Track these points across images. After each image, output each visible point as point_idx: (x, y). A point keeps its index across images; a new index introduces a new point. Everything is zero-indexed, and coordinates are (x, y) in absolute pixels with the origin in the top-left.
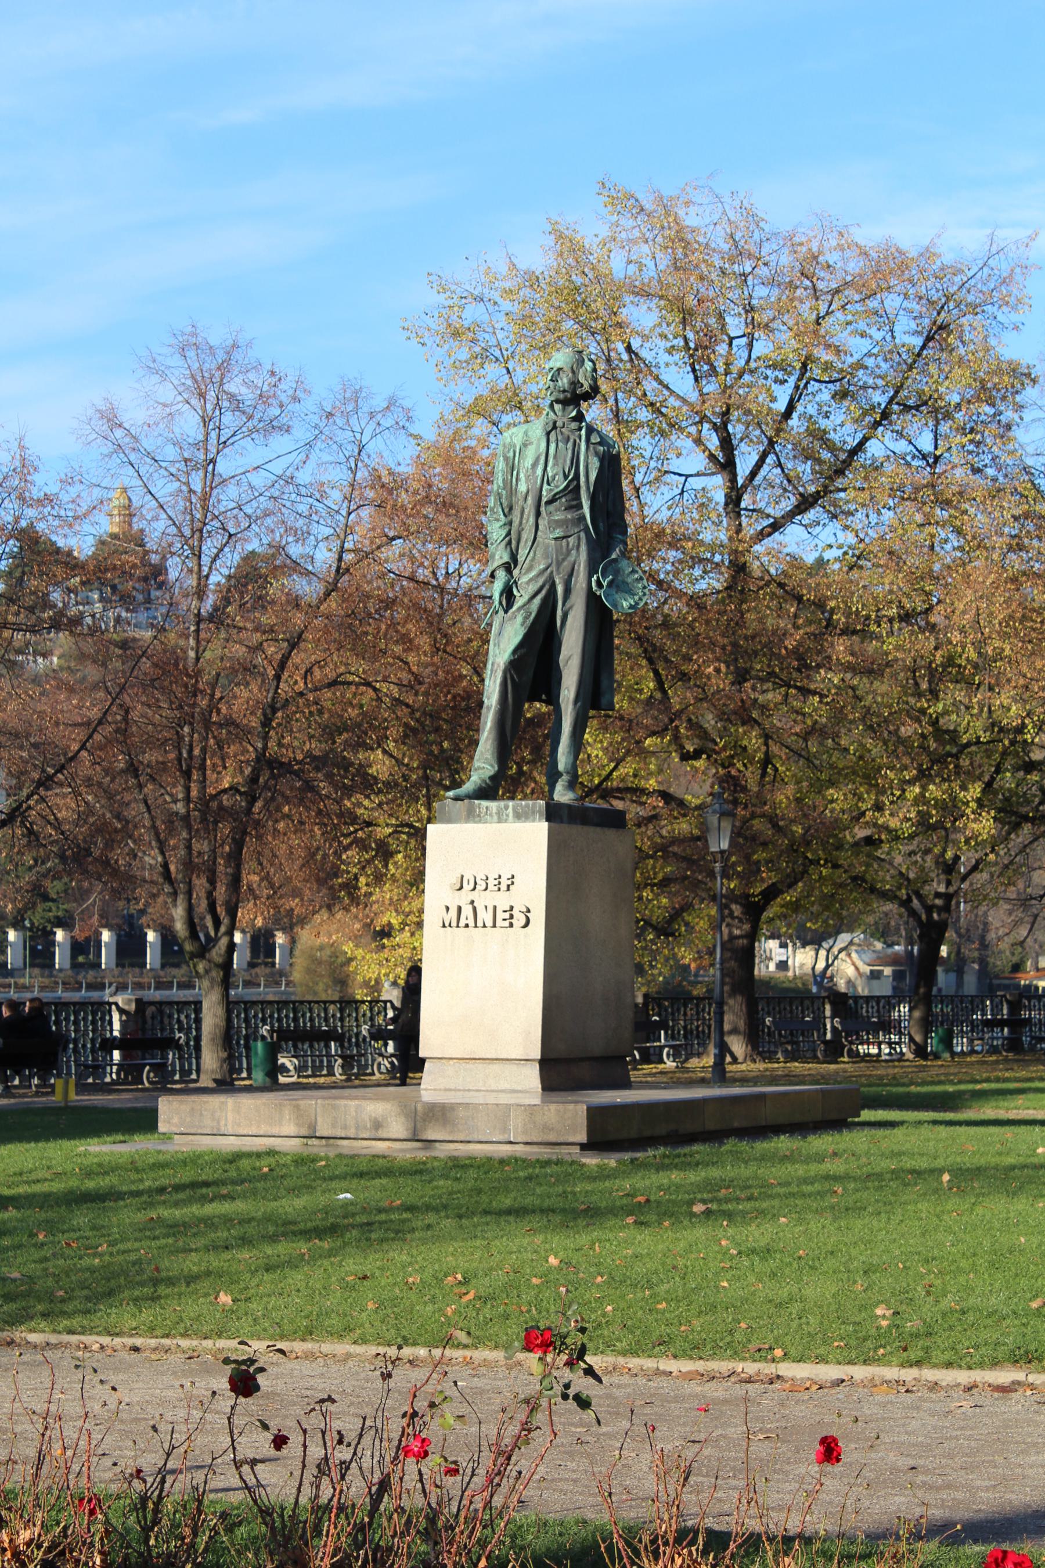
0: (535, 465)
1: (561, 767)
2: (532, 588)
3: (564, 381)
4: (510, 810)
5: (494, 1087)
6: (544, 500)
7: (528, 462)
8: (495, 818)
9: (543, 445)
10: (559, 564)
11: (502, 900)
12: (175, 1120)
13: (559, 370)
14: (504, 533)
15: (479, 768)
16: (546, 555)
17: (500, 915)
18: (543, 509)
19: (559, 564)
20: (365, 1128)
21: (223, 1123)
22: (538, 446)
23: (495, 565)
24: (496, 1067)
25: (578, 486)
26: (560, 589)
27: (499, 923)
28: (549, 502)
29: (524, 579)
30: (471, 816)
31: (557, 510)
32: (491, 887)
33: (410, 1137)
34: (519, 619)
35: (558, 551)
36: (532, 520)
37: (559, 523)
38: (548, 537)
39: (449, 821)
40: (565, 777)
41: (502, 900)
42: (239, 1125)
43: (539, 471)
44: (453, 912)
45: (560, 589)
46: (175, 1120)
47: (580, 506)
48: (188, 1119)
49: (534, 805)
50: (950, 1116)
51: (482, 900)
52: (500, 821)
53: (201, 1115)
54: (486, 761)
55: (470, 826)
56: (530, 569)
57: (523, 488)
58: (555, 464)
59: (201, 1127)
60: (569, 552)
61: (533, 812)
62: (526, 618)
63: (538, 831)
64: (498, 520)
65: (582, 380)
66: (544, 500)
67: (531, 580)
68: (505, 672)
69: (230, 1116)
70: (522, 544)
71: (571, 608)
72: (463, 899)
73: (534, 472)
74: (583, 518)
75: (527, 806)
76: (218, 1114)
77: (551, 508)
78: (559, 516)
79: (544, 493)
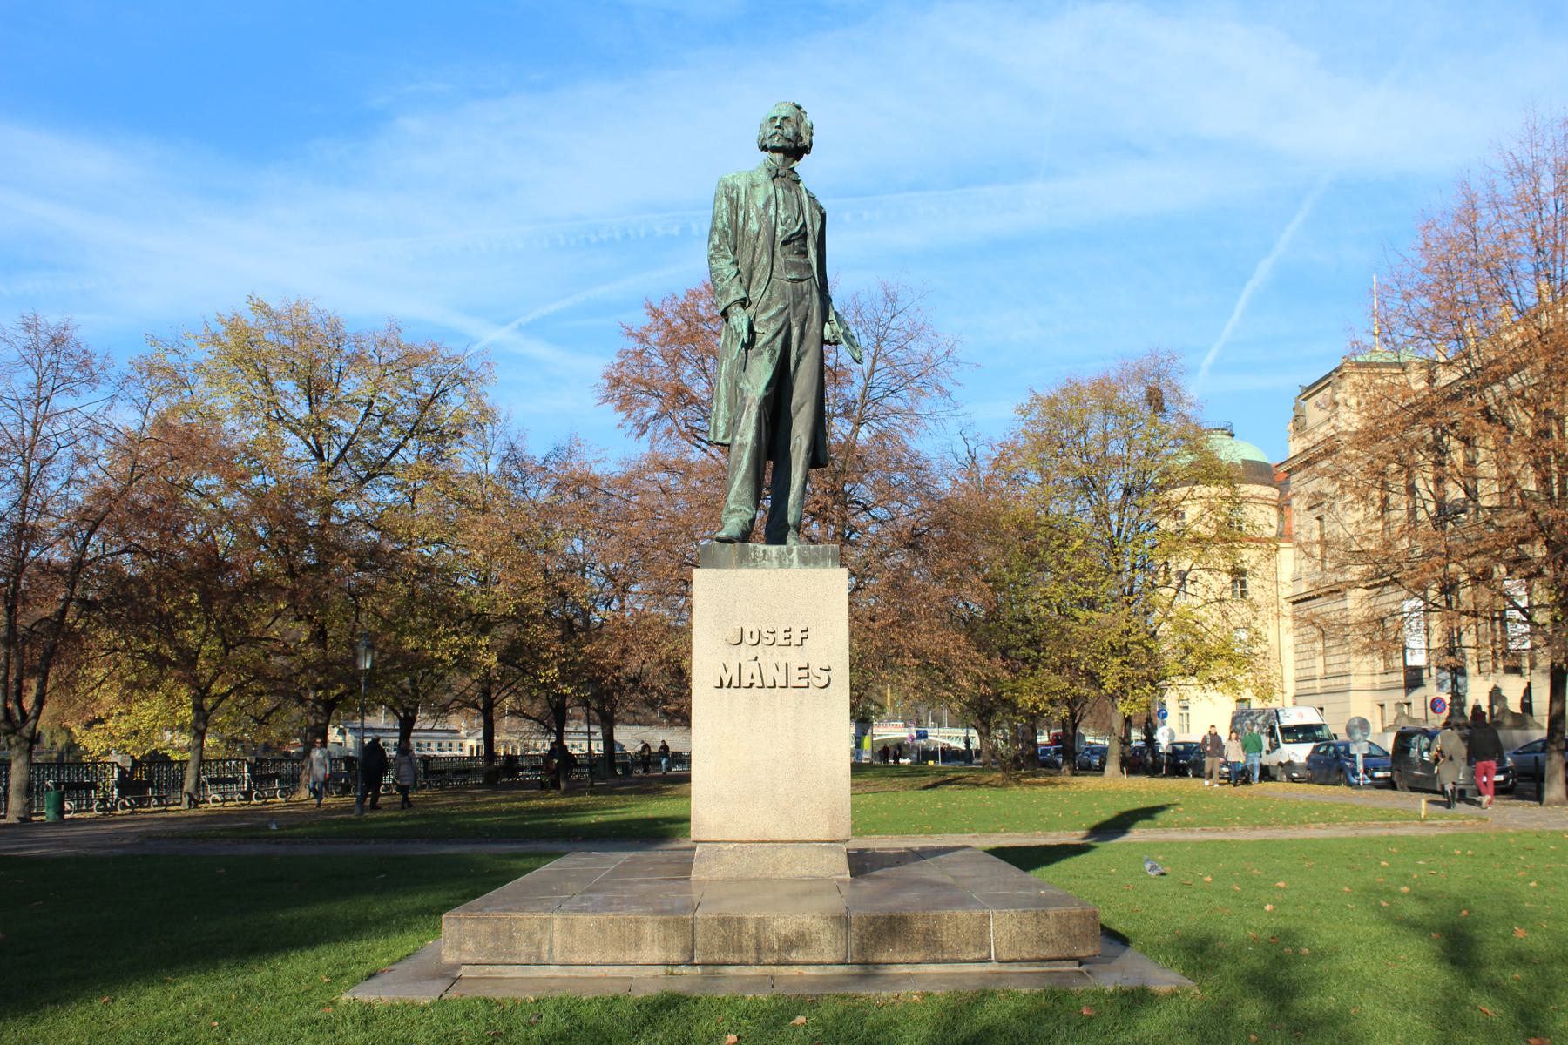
0: (767, 205)
1: (791, 519)
2: (774, 327)
3: (789, 131)
4: (795, 554)
5: (790, 873)
6: (779, 241)
7: (760, 202)
8: (776, 562)
9: (771, 189)
10: (795, 306)
11: (795, 658)
12: (470, 945)
13: (785, 118)
14: (734, 270)
15: (735, 511)
16: (783, 296)
17: (795, 674)
18: (778, 249)
19: (795, 306)
20: (772, 950)
21: (545, 948)
22: (767, 189)
23: (731, 300)
24: (790, 850)
25: (805, 235)
26: (795, 332)
27: (794, 681)
28: (785, 243)
29: (764, 317)
30: (744, 560)
31: (791, 252)
32: (781, 641)
33: (841, 959)
34: (766, 356)
35: (795, 292)
36: (765, 259)
37: (794, 266)
38: (784, 276)
39: (716, 566)
40: (792, 530)
41: (795, 658)
42: (572, 950)
43: (772, 211)
44: (734, 672)
45: (795, 332)
46: (470, 945)
47: (805, 254)
48: (490, 945)
49: (825, 549)
50: (395, 823)
51: (771, 658)
52: (781, 565)
53: (511, 938)
54: (743, 503)
55: (744, 571)
56: (766, 308)
57: (754, 226)
58: (786, 208)
59: (512, 955)
60: (803, 295)
61: (824, 558)
62: (772, 355)
63: (837, 581)
64: (726, 257)
65: (803, 133)
66: (779, 241)
67: (770, 318)
68: (760, 408)
69: (557, 938)
70: (754, 283)
71: (805, 353)
72: (745, 653)
73: (766, 212)
74: (810, 266)
75: (816, 550)
76: (538, 936)
77: (786, 249)
78: (793, 259)
79: (779, 233)
